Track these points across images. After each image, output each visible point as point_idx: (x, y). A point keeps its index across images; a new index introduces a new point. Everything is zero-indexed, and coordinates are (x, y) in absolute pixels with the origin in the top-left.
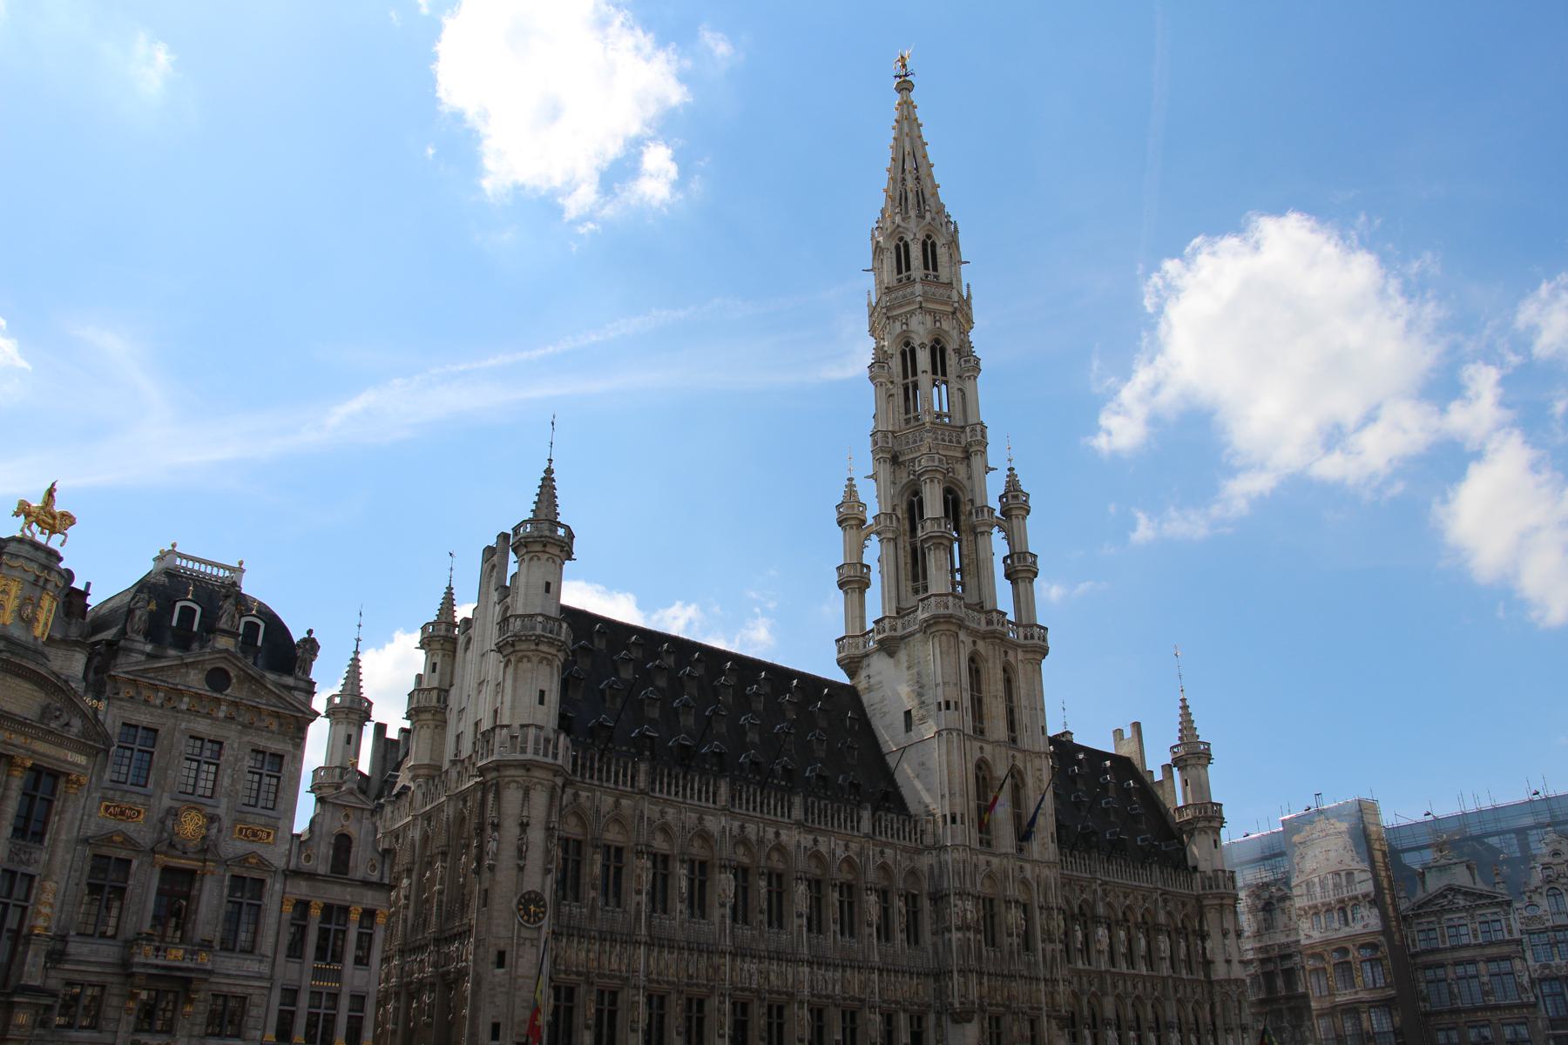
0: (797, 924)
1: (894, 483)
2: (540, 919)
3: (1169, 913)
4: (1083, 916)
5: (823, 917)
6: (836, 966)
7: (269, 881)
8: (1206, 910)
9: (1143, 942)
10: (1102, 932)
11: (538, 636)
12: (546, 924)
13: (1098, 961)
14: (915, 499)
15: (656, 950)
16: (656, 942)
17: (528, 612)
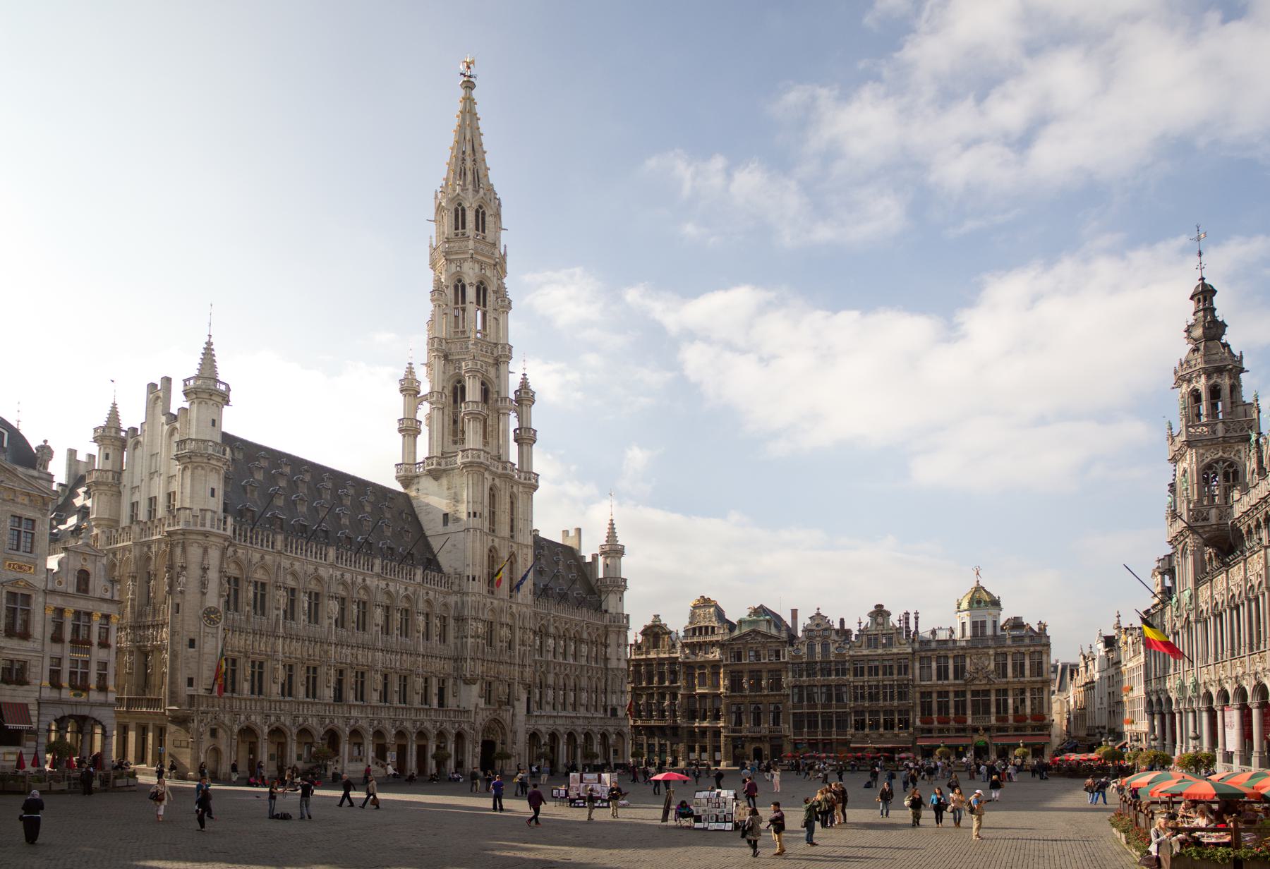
0: (374, 630)
1: (444, 373)
2: (218, 623)
3: (589, 634)
4: (542, 633)
5: (390, 625)
6: (397, 652)
7: (34, 596)
8: (610, 633)
9: (573, 647)
10: (551, 641)
11: (210, 455)
12: (221, 625)
13: (547, 656)
14: (459, 385)
15: (289, 640)
16: (289, 637)
17: (200, 437)
